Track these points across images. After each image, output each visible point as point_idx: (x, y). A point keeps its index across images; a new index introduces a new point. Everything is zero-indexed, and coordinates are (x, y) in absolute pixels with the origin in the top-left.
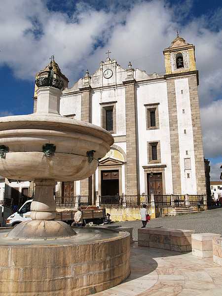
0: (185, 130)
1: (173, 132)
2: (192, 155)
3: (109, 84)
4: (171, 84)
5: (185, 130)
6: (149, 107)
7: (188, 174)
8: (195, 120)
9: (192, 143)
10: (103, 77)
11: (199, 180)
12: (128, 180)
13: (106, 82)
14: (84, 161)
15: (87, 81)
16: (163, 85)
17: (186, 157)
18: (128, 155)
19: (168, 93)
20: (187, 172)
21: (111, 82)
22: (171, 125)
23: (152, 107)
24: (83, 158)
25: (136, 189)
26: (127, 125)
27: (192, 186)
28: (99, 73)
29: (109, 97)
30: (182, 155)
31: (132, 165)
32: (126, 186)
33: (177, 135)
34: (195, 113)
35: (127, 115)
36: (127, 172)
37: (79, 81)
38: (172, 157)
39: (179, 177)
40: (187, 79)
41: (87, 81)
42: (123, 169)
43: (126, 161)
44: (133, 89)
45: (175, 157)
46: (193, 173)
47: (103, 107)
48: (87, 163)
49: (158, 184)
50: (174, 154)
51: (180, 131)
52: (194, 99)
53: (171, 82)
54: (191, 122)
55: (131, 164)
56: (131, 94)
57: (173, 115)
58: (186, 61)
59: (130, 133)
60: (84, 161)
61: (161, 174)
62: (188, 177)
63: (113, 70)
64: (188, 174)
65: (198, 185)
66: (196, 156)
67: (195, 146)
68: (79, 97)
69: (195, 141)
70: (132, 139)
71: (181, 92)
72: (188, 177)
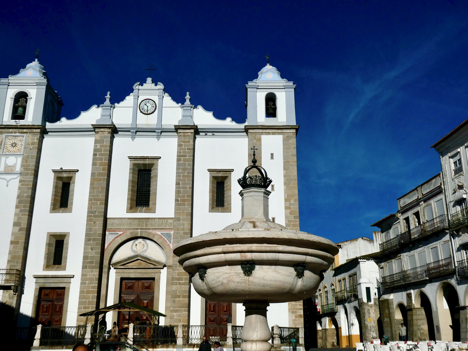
6: (216, 174)
23: (220, 175)
36: (170, 282)
47: (134, 164)
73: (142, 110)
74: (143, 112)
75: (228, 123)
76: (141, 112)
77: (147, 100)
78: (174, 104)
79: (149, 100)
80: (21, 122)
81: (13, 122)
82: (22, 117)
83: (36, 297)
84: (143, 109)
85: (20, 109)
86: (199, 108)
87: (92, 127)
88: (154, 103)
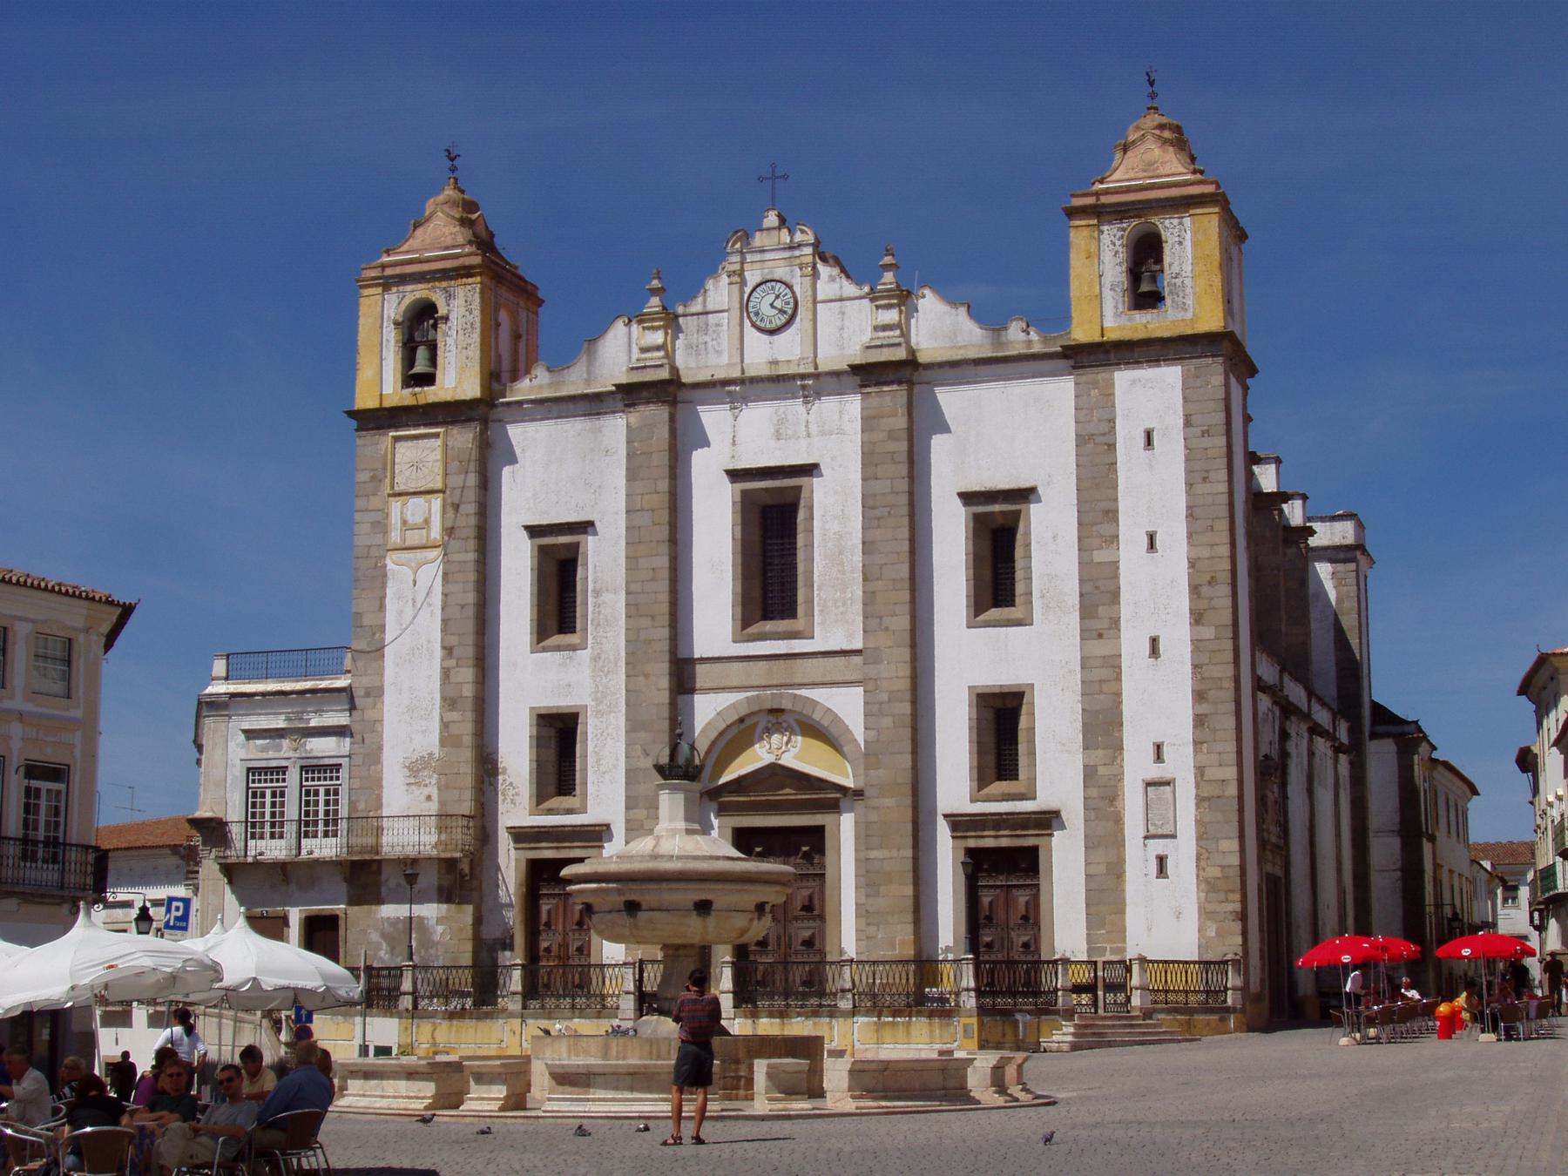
0: (1154, 641)
1: (1099, 648)
2: (1181, 764)
3: (775, 363)
4: (1094, 393)
5: (1154, 641)
7: (1161, 860)
8: (1205, 590)
9: (1184, 708)
10: (747, 323)
11: (1208, 885)
12: (869, 879)
13: (760, 354)
14: (751, 920)
15: (658, 337)
16: (1061, 391)
17: (1155, 772)
18: (871, 757)
19: (1081, 440)
20: (1157, 846)
21: (788, 350)
22: (1087, 610)
24: (750, 916)
25: (910, 928)
26: (869, 600)
27: (1178, 915)
28: (719, 293)
29: (778, 436)
30: (1136, 766)
31: (895, 808)
32: (862, 912)
33: (1113, 664)
34: (1205, 553)
35: (868, 546)
36: (865, 838)
37: (610, 335)
38: (1090, 773)
39: (1117, 871)
40: (1179, 369)
41: (658, 337)
42: (845, 829)
43: (861, 784)
44: (902, 411)
45: (1102, 770)
46: (1184, 852)
48: (756, 922)
49: (1022, 898)
50: (1098, 755)
51: (1132, 643)
52: (1205, 479)
53: (1095, 384)
54: (1182, 603)
55: (889, 802)
56: (892, 435)
57: (1099, 556)
58: (1175, 269)
59: (883, 640)
60: (751, 920)
61: (1033, 852)
62: (1162, 871)
63: (800, 285)
64: (1161, 860)
65: (1205, 914)
66: (1200, 771)
67: (1199, 721)
68: (616, 427)
69: (1199, 696)
70: (895, 671)
71: (1142, 441)
72: (1162, 871)
73: (754, 319)
74: (758, 323)
75: (1018, 337)
76: (754, 325)
77: (769, 284)
78: (850, 289)
79: (774, 283)
80: (431, 394)
81: (406, 397)
82: (428, 379)
83: (521, 885)
84: (757, 314)
85: (422, 354)
86: (924, 297)
87: (614, 388)
88: (788, 290)
